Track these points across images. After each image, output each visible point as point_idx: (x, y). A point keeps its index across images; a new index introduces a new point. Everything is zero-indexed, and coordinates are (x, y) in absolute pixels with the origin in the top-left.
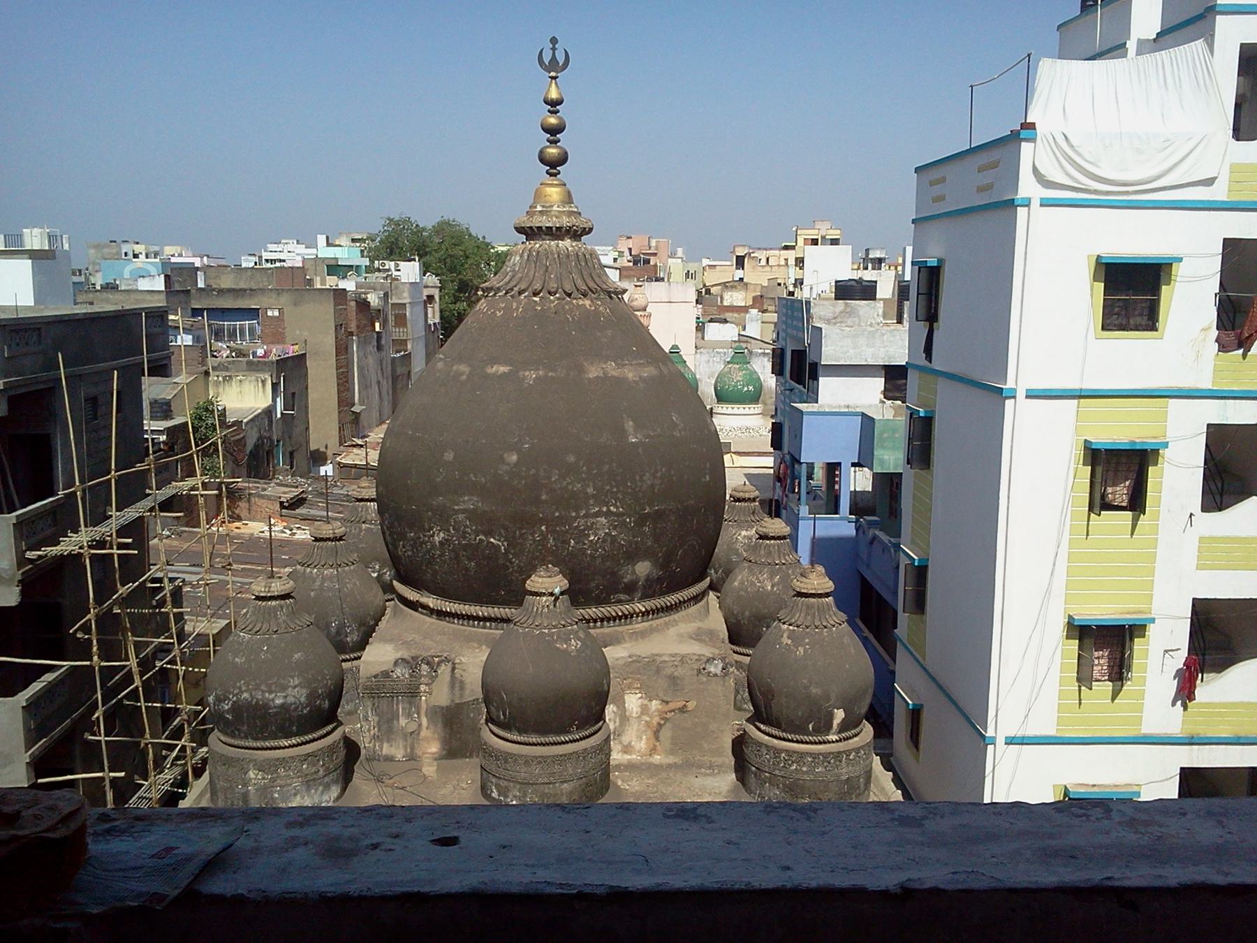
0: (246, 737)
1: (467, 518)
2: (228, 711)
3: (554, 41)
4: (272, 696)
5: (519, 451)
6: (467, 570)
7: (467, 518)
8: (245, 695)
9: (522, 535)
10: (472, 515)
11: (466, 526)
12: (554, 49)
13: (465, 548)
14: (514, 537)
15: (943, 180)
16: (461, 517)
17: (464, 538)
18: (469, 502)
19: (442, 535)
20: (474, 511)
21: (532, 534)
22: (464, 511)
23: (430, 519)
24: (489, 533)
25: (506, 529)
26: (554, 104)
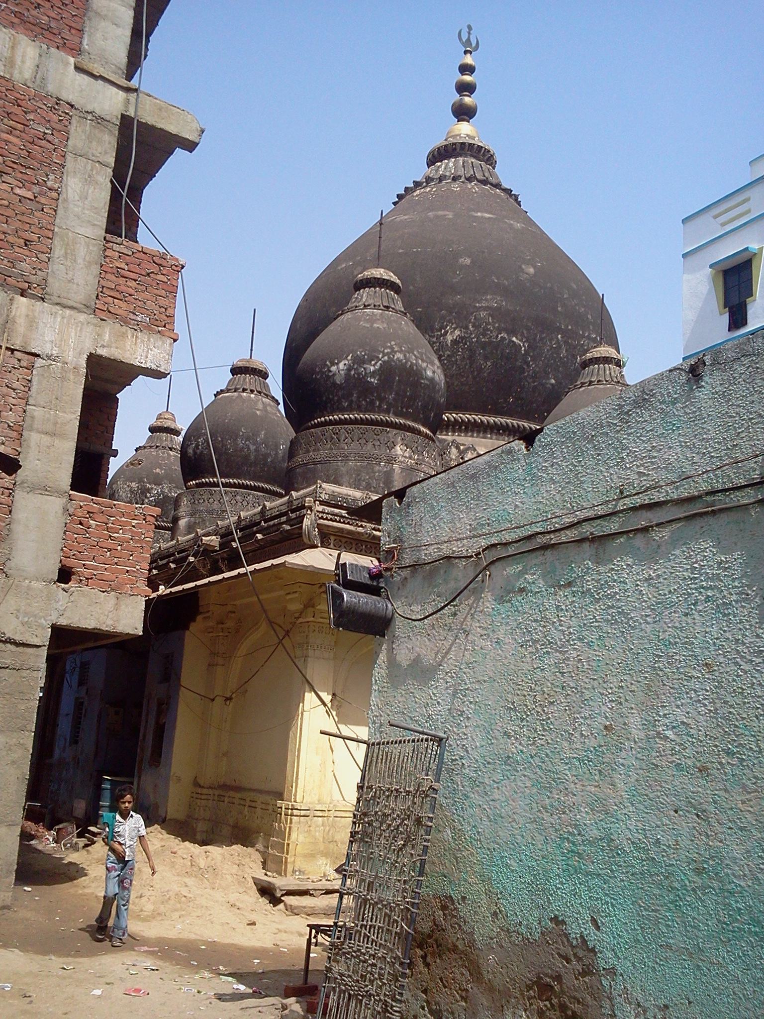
0: (387, 411)
1: (490, 315)
2: (373, 374)
3: (470, 27)
4: (424, 365)
5: (535, 267)
6: (480, 370)
7: (490, 315)
8: (399, 356)
9: (541, 339)
10: (495, 313)
11: (488, 324)
12: (469, 33)
13: (484, 346)
14: (535, 339)
15: (747, 200)
16: (483, 314)
17: (484, 335)
18: (492, 301)
19: (457, 332)
20: (498, 309)
21: (551, 340)
22: (485, 309)
23: (443, 318)
24: (513, 332)
25: (528, 330)
26: (466, 69)
